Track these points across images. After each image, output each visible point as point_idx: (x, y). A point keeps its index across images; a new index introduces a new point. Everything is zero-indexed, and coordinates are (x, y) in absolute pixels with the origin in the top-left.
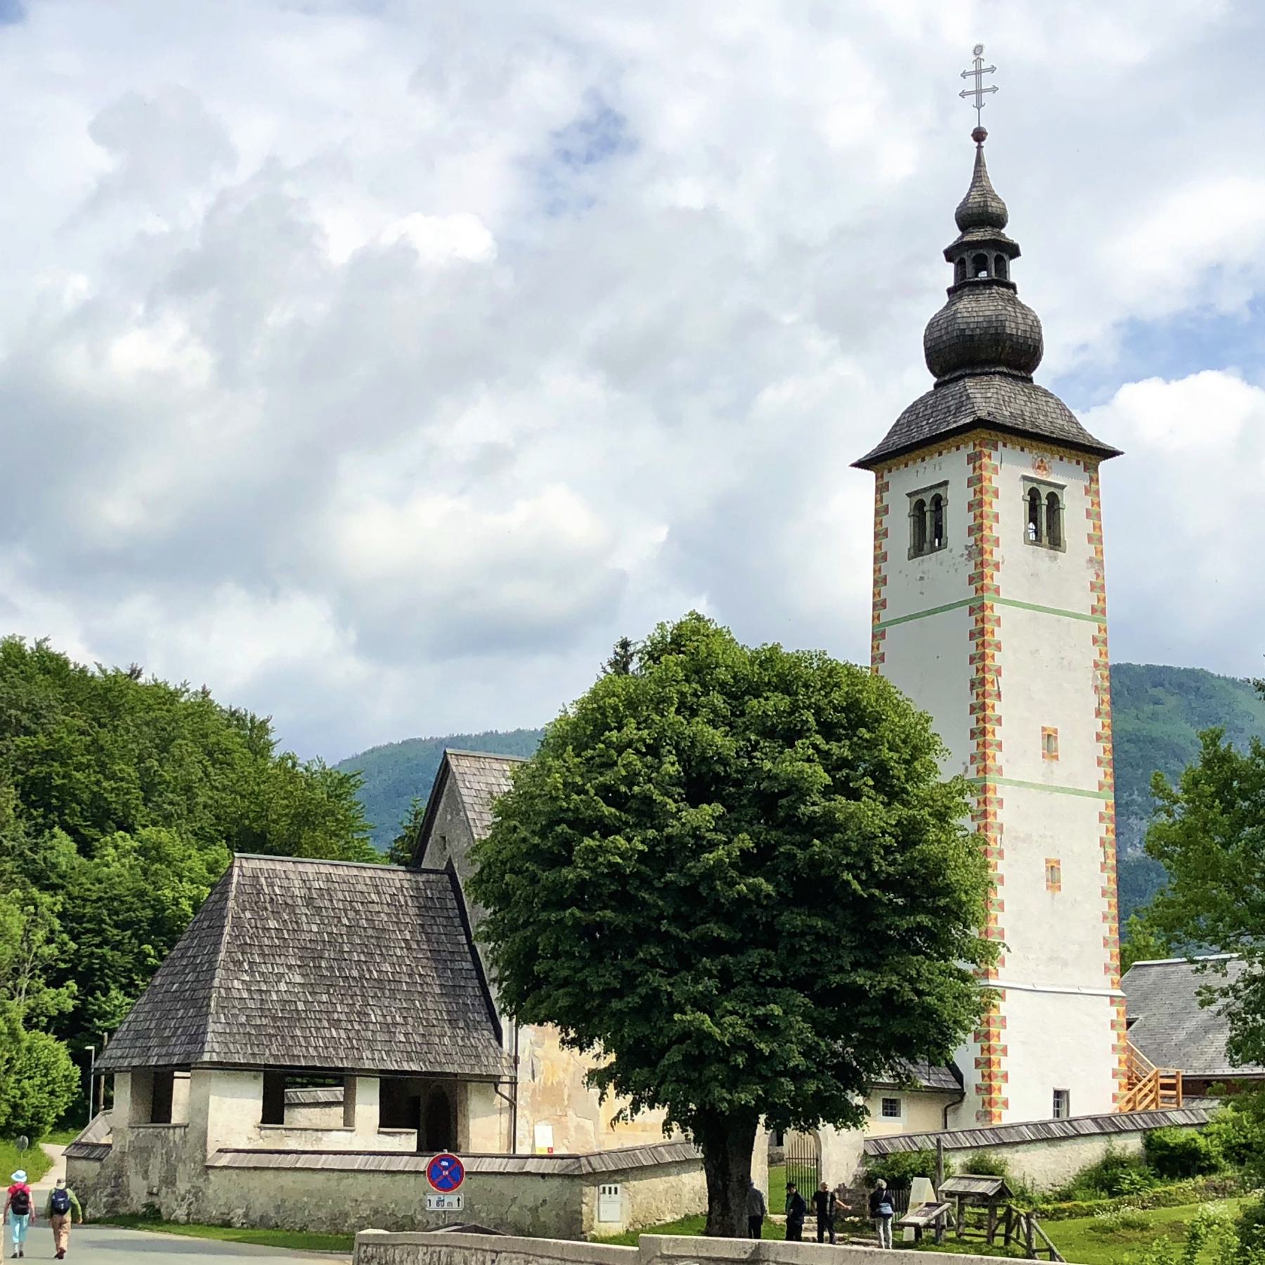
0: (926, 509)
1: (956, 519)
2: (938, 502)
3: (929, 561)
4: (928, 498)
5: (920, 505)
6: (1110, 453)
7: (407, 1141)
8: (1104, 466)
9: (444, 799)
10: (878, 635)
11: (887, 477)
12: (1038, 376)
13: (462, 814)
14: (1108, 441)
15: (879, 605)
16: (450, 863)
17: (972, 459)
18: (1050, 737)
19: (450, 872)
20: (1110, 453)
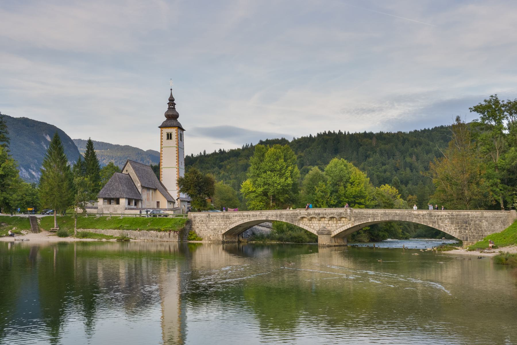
0: (169, 135)
1: (174, 136)
2: (171, 134)
3: (169, 141)
4: (169, 133)
5: (168, 134)
6: (185, 130)
7: (135, 207)
8: (184, 131)
9: (127, 165)
10: (161, 148)
11: (162, 129)
12: (179, 120)
13: (131, 168)
14: (184, 129)
15: (161, 145)
16: (128, 173)
17: (176, 130)
18: (182, 162)
19: (128, 174)
20: (185, 130)
